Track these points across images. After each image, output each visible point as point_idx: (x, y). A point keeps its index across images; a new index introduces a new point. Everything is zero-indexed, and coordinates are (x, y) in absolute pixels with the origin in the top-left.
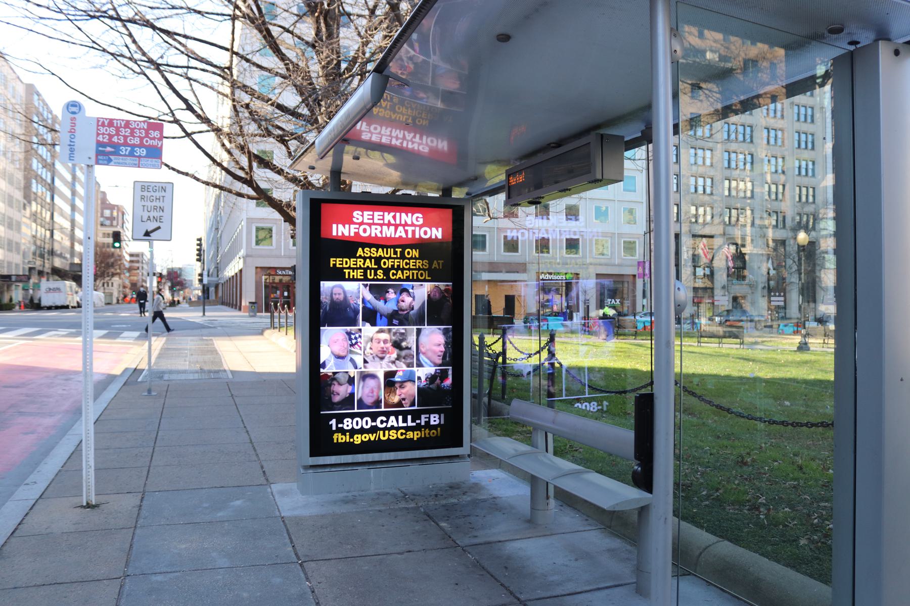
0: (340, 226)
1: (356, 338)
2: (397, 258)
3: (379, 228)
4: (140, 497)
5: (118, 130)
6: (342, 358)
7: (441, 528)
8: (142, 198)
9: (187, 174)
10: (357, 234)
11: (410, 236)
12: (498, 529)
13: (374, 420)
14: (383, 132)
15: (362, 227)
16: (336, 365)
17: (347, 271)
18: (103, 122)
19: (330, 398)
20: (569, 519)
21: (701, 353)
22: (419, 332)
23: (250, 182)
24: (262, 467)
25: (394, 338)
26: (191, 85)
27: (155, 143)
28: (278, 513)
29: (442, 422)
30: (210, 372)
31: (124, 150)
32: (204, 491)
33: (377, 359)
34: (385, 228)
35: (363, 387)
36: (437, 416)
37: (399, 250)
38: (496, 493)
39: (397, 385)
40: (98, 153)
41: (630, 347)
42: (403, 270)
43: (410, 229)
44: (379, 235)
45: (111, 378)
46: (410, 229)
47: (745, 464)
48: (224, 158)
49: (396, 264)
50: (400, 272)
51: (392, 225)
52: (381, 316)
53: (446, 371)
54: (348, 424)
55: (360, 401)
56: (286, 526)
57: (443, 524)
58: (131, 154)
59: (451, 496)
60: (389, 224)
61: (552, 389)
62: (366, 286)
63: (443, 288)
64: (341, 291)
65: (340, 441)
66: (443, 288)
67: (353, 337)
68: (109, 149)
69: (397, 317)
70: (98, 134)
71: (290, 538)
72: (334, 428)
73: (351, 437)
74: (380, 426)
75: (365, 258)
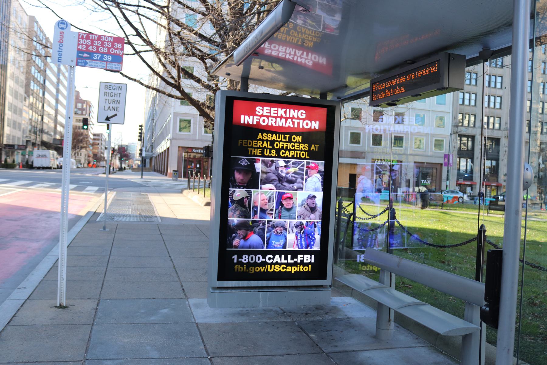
0: (247, 117)
2: (286, 142)
3: (274, 119)
4: (96, 303)
5: (92, 41)
7: (311, 339)
8: (105, 94)
9: (135, 80)
10: (258, 123)
11: (296, 126)
12: (352, 342)
13: (264, 257)
14: (280, 50)
15: (263, 118)
18: (83, 36)
20: (404, 337)
23: (178, 87)
24: (182, 286)
26: (140, 19)
27: (118, 52)
28: (193, 320)
29: (313, 261)
30: (146, 217)
31: (96, 56)
32: (141, 301)
34: (278, 119)
36: (309, 256)
37: (287, 136)
38: (350, 315)
40: (79, 58)
41: (439, 214)
43: (296, 121)
44: (274, 125)
45: (78, 218)
46: (296, 121)
47: (535, 305)
48: (160, 69)
49: (285, 146)
50: (287, 152)
51: (284, 118)
56: (199, 330)
57: (312, 335)
58: (101, 60)
59: (317, 315)
60: (281, 117)
65: (239, 270)
68: (86, 55)
70: (79, 45)
71: (202, 339)
72: (235, 261)
73: (247, 268)
74: (268, 261)
75: (263, 141)
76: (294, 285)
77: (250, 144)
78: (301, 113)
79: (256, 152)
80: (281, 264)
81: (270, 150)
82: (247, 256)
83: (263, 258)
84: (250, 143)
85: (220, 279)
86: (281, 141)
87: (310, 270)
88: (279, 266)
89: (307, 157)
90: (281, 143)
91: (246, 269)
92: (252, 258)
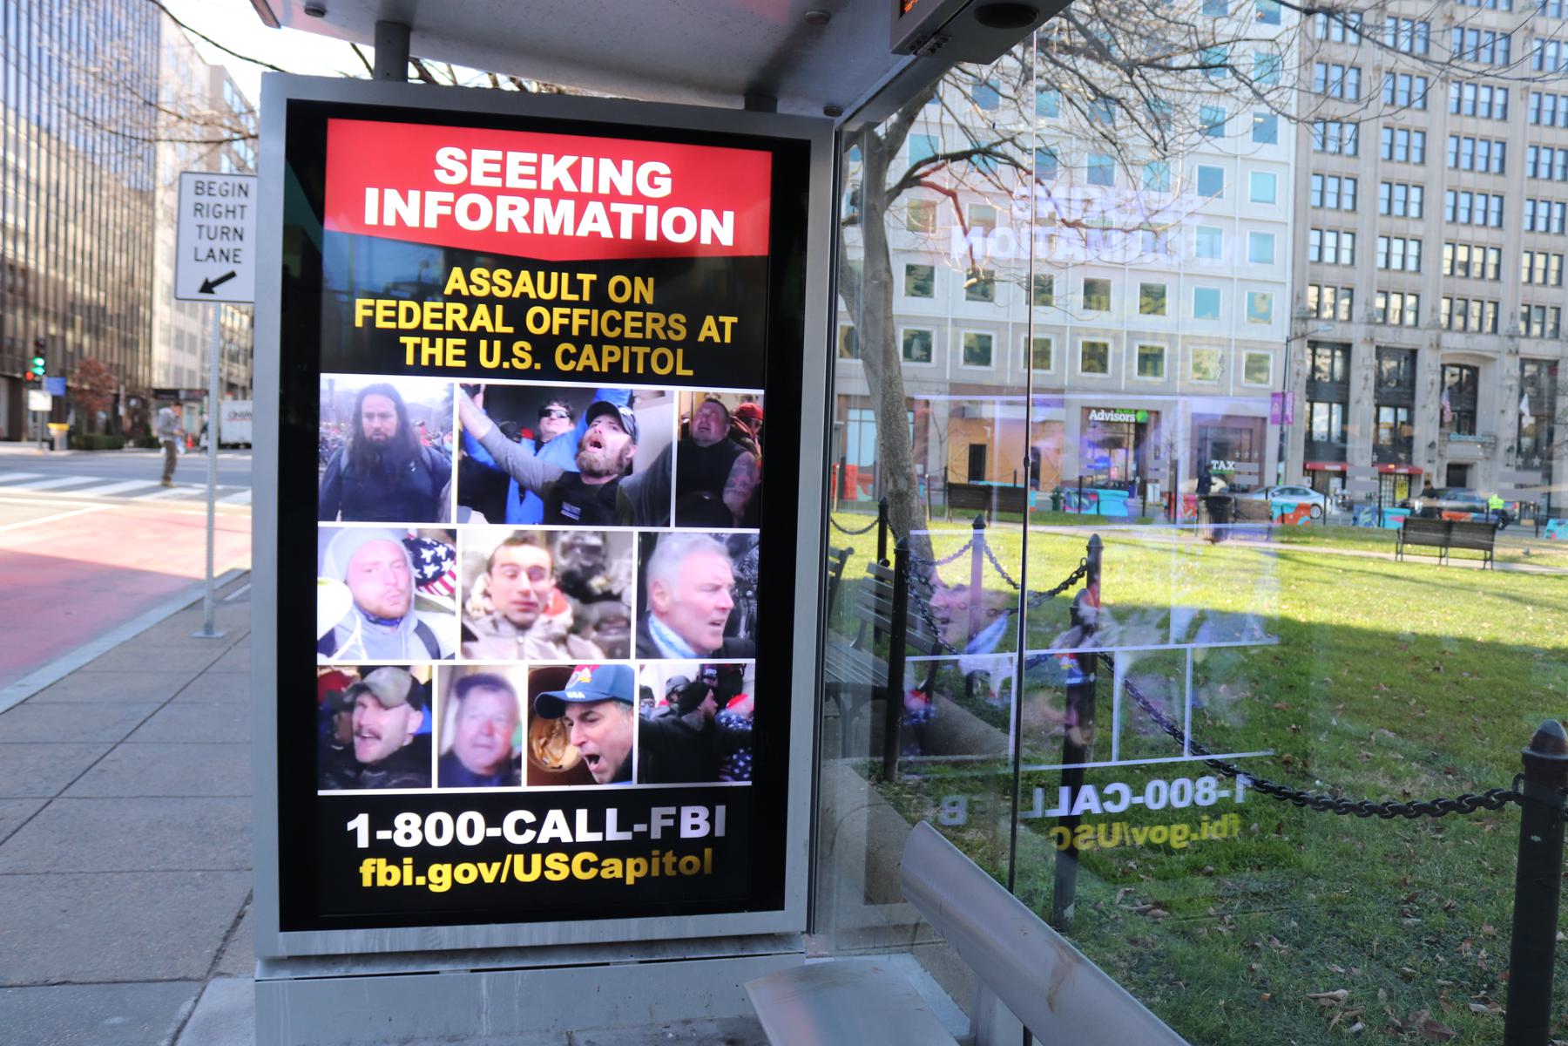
0: (392, 195)
1: (436, 560)
2: (580, 304)
3: (522, 204)
6: (392, 621)
8: (198, 209)
10: (447, 222)
11: (626, 233)
13: (494, 820)
15: (468, 199)
16: (368, 642)
17: (410, 342)
19: (350, 749)
21: (1412, 580)
22: (648, 545)
25: (564, 562)
29: (720, 831)
33: (506, 628)
34: (542, 205)
35: (459, 717)
36: (703, 812)
37: (587, 278)
39: (572, 714)
41: (1262, 558)
42: (599, 342)
43: (627, 212)
44: (522, 228)
46: (627, 212)
49: (577, 322)
50: (588, 349)
51: (568, 196)
52: (522, 490)
53: (735, 673)
54: (407, 830)
55: (450, 761)
60: (557, 194)
61: (1077, 736)
62: (472, 391)
63: (733, 406)
64: (390, 407)
65: (382, 881)
66: (733, 406)
67: (427, 555)
69: (578, 497)
72: (363, 842)
73: (420, 870)
74: (513, 838)
75: (472, 302)
76: (634, 937)
77: (409, 317)
78: (652, 175)
79: (438, 351)
80: (572, 849)
81: (507, 341)
82: (415, 818)
83: (489, 824)
84: (410, 315)
85: (291, 920)
86: (558, 302)
87: (708, 870)
88: (563, 857)
89: (680, 372)
90: (557, 311)
91: (415, 874)
92: (439, 825)
